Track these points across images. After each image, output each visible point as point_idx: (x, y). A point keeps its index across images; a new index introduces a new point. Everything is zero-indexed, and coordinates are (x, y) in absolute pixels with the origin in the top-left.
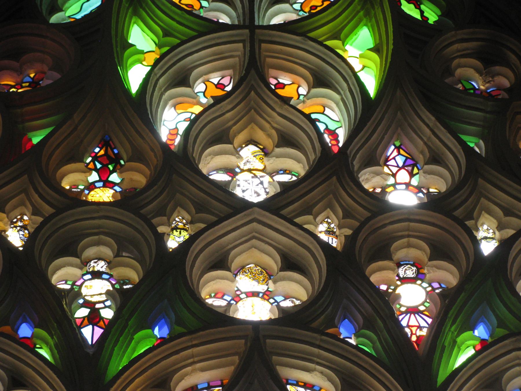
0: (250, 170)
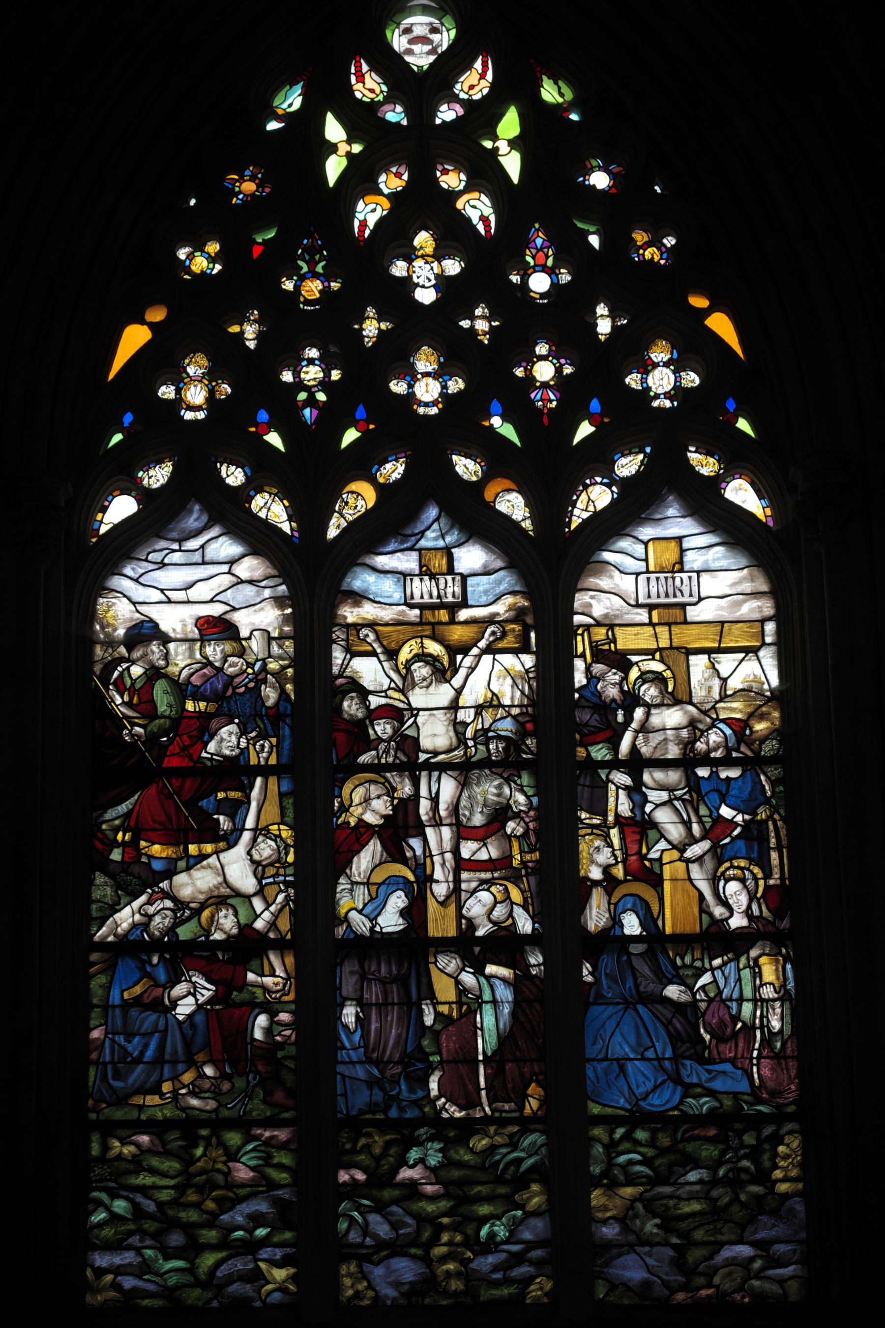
0: (422, 257)
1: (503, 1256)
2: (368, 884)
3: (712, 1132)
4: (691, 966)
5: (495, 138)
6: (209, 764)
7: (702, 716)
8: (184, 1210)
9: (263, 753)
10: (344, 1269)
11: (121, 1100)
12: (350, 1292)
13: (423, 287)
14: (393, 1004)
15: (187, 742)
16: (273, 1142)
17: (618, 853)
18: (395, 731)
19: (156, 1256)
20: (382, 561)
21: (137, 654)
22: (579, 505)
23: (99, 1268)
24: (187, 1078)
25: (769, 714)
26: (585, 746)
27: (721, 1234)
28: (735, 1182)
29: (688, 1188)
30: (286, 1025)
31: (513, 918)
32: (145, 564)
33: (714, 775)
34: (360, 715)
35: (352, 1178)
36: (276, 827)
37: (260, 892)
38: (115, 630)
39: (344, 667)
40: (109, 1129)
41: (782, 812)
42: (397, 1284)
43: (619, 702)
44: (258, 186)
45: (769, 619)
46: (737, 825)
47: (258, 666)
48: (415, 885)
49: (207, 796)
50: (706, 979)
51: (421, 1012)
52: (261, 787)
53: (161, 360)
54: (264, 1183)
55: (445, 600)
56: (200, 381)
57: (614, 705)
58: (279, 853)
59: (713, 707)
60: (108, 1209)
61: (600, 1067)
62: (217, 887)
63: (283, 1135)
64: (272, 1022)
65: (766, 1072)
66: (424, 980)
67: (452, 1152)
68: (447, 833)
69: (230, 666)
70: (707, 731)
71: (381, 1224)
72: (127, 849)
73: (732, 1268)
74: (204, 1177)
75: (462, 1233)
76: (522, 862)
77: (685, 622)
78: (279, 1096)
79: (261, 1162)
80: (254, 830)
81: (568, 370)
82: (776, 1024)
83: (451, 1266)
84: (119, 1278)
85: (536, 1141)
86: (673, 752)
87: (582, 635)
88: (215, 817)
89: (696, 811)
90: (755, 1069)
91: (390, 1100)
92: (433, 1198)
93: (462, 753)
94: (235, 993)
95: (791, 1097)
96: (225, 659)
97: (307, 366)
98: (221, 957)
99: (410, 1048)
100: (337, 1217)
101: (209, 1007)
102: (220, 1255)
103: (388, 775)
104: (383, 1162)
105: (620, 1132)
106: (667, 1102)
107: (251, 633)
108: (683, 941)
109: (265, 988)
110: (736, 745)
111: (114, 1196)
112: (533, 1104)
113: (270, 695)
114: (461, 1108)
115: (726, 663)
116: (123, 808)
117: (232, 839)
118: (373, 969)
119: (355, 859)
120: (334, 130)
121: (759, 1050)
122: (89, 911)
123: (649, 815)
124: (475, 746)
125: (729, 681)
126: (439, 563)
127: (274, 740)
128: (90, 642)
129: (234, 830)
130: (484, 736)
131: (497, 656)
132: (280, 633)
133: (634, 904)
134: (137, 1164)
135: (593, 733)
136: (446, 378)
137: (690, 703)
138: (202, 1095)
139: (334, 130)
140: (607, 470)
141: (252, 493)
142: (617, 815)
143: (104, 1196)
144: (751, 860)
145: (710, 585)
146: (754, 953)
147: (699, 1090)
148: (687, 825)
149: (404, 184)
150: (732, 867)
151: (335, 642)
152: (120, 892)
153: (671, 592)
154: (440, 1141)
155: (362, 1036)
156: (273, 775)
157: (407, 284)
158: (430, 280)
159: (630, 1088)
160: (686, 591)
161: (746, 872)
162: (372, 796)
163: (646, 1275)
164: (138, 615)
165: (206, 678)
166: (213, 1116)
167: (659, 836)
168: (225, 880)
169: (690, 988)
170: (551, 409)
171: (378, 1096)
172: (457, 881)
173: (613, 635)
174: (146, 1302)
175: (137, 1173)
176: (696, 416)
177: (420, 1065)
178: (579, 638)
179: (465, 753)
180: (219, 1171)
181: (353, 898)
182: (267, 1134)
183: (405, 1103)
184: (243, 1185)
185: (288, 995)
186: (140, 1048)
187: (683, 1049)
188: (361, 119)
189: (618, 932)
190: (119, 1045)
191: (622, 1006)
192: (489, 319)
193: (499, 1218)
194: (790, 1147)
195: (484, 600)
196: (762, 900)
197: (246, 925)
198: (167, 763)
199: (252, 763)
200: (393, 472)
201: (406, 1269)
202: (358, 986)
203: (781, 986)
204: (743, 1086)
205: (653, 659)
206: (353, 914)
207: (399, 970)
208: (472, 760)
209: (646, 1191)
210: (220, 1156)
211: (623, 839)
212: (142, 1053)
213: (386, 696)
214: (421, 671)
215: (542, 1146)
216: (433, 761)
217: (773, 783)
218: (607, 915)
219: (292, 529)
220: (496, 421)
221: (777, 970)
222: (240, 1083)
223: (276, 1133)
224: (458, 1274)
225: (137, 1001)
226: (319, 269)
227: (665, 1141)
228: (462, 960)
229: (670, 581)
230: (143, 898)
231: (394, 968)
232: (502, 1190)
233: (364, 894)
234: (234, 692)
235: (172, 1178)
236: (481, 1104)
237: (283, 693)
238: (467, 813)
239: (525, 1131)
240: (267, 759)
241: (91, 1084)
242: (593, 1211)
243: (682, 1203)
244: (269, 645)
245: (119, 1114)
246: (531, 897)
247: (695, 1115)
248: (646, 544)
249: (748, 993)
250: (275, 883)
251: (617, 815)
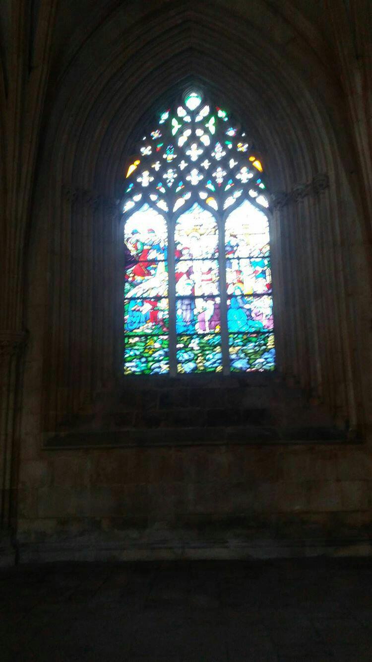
3: (255, 335)
9: (161, 257)
11: (132, 331)
12: (179, 371)
28: (260, 346)
40: (129, 337)
63: (166, 337)
92: (197, 350)
108: (249, 296)
113: (162, 245)
134: (135, 344)
139: (174, 122)
174: (137, 373)
176: (252, 184)
188: (180, 120)
194: (271, 340)
198: (142, 259)
201: (191, 365)
225: (134, 310)
227: (245, 337)
239: (216, 336)
245: (131, 334)
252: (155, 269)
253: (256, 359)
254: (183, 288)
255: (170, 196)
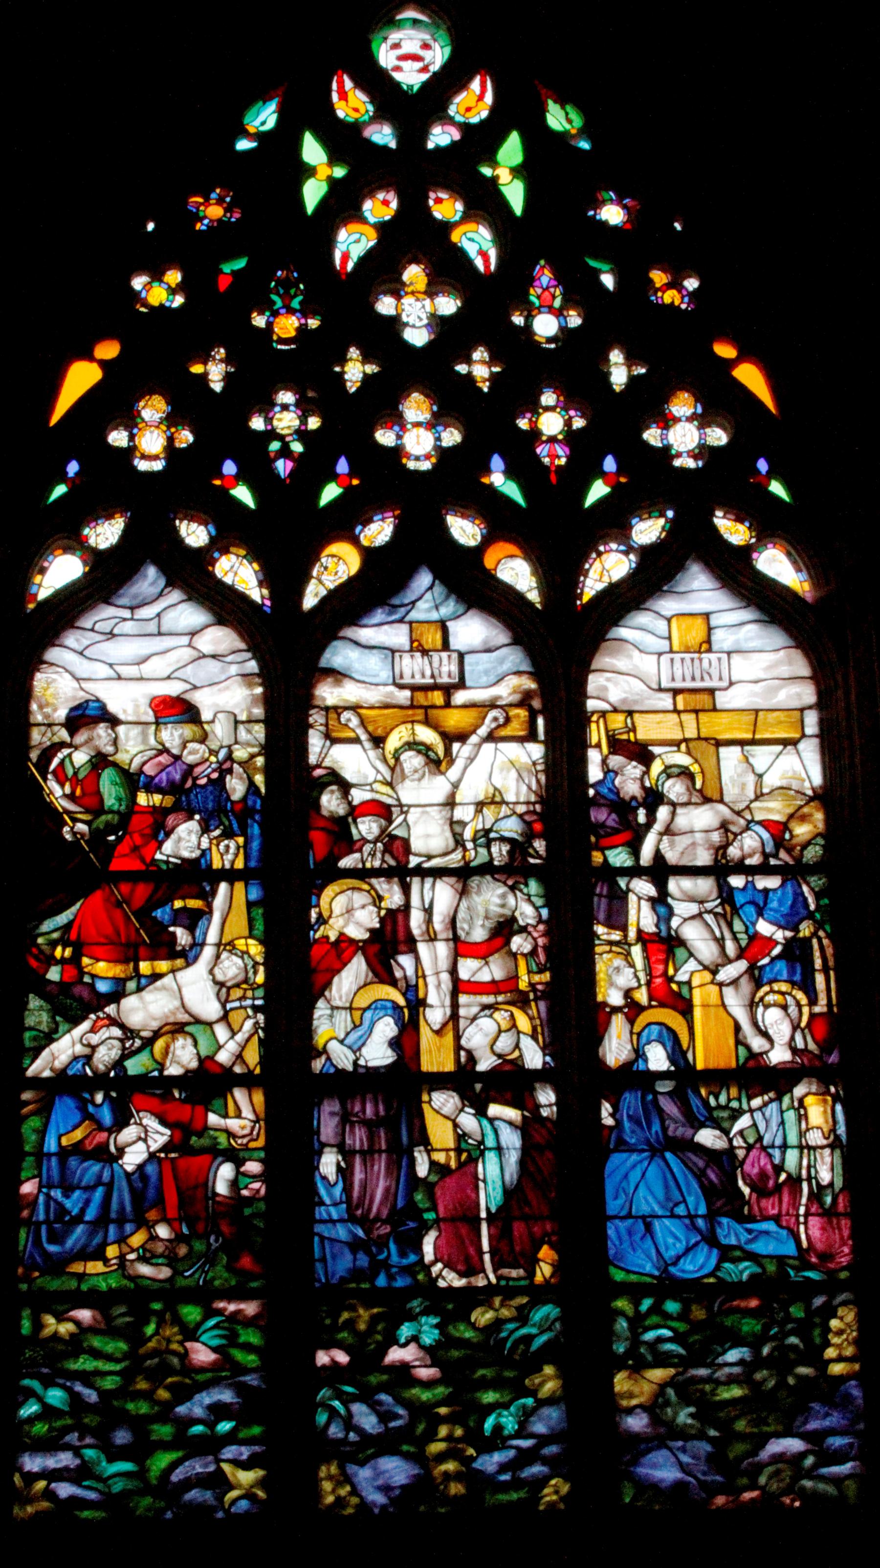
0: (413, 293)
1: (512, 1453)
2: (351, 1008)
3: (754, 1303)
4: (726, 1107)
5: (494, 164)
6: (164, 867)
7: (735, 818)
8: (132, 1401)
9: (227, 854)
10: (323, 1472)
11: (57, 1266)
12: (330, 1499)
13: (413, 326)
14: (380, 1152)
15: (138, 840)
16: (240, 1317)
17: (642, 976)
18: (383, 831)
19: (98, 1458)
20: (365, 634)
21: (80, 738)
22: (591, 574)
23: (29, 1472)
24: (137, 1239)
25: (811, 815)
26: (602, 850)
27: (768, 1425)
28: (782, 1362)
29: (727, 1370)
30: (255, 1177)
31: (520, 1050)
32: (91, 634)
33: (749, 885)
34: (341, 810)
35: (333, 1360)
36: (243, 941)
37: (225, 1018)
38: (55, 710)
39: (323, 755)
41: (828, 928)
42: (386, 1489)
43: (640, 800)
44: (226, 210)
45: (810, 707)
46: (776, 943)
47: (222, 754)
48: (406, 1011)
49: (161, 904)
50: (744, 1122)
51: (412, 1162)
52: (226, 896)
53: (112, 402)
54: (228, 1366)
55: (439, 681)
56: (157, 427)
57: (634, 804)
58: (247, 972)
59: (748, 807)
60: (40, 1400)
61: (623, 1225)
62: (174, 1014)
63: (250, 1308)
64: (238, 1173)
65: (816, 1233)
66: (417, 1122)
67: (451, 1327)
68: (443, 949)
69: (190, 753)
70: (741, 834)
71: (367, 1415)
72: (67, 967)
73: (780, 1466)
74: (156, 1360)
75: (464, 1425)
76: (532, 985)
77: (715, 709)
78: (246, 1262)
79: (224, 1342)
80: (218, 945)
81: (579, 423)
82: (825, 1176)
83: (450, 1466)
84: (53, 1485)
85: (549, 1314)
86: (704, 858)
87: (597, 722)
88: (172, 929)
89: (730, 925)
90: (802, 1228)
91: (378, 1266)
93: (460, 856)
94: (194, 1138)
95: (844, 1261)
96: (184, 746)
97: (281, 412)
98: (177, 1095)
99: (400, 1203)
100: (313, 1407)
101: (163, 1155)
102: (173, 1456)
103: (374, 881)
104: (369, 1341)
105: (646, 1304)
106: (701, 1268)
107: (215, 716)
108: (717, 1078)
109: (230, 1134)
110: (774, 851)
111: (48, 1383)
112: (544, 1271)
114: (462, 1275)
115: (762, 756)
116: (62, 919)
117: (191, 955)
118: (357, 1108)
119: (336, 980)
120: (312, 151)
121: (807, 1206)
122: (22, 1040)
123: (676, 931)
124: (475, 849)
125: (765, 778)
126: (433, 638)
127: (241, 840)
128: (25, 724)
129: (194, 945)
130: (485, 837)
131: (501, 745)
132: (248, 716)
133: (660, 1034)
134: (75, 1345)
135: (608, 835)
136: (440, 428)
137: (721, 801)
138: (154, 1261)
139: (312, 151)
140: (623, 533)
141: (216, 555)
142: (640, 932)
143: (35, 1384)
144: (793, 983)
145: (741, 668)
146: (799, 1091)
147: (738, 1253)
148: (720, 942)
149: (393, 213)
150: (772, 991)
151: (311, 726)
152: (58, 1018)
153: (698, 675)
154: (436, 1315)
155: (344, 1190)
156: (239, 880)
157: (394, 325)
158: (421, 319)
159: (658, 1252)
160: (715, 675)
161: (788, 998)
162: (356, 906)
163: (679, 1475)
164: (82, 693)
165: (161, 768)
166: (167, 1285)
167: (686, 954)
168: (183, 1005)
169: (726, 1132)
170: (559, 466)
171: (363, 1260)
172: (455, 1006)
173: (633, 723)
174: (86, 1514)
175: (76, 1356)
177: (412, 1225)
178: (593, 726)
179: (464, 857)
180: (175, 1353)
181: (333, 1025)
182: (232, 1307)
183: (394, 1270)
184: (202, 1369)
185: (256, 1140)
186: (80, 1205)
187: (719, 1204)
188: (343, 140)
189: (641, 1066)
190: (56, 1201)
191: (646, 1154)
192: (489, 364)
193: (506, 1406)
194: (843, 1321)
195: (484, 680)
196: (806, 1031)
197: (208, 1057)
198: (116, 865)
199: (215, 867)
200: (379, 533)
201: (396, 1470)
202: (339, 1130)
203: (830, 1131)
204: (790, 1249)
205: (679, 750)
206: (334, 1047)
207: (386, 1109)
208: (473, 864)
209: (677, 1374)
210: (175, 1334)
211: (647, 958)
212: (83, 1211)
213: (372, 790)
214: (412, 761)
215: (556, 1320)
216: (426, 865)
217: (818, 896)
218: (629, 1047)
219: (263, 597)
220: (498, 479)
221: (825, 1112)
222: (199, 1246)
223: (242, 1306)
224: (457, 1477)
225: (77, 1149)
226: (295, 304)
227: (699, 1313)
228: (462, 1098)
229: (697, 662)
230: (86, 1025)
231: (381, 1107)
232: (509, 1374)
233: (346, 1021)
234: (195, 785)
235: (118, 1361)
236: (483, 1271)
237: (252, 784)
238: (466, 926)
240: (233, 862)
241: (21, 1248)
242: (617, 1398)
243: (721, 1389)
244: (236, 729)
245: (55, 1285)
246: (541, 1025)
247: (733, 1283)
248: (669, 620)
249: (792, 1139)
250: (241, 1007)
251: (640, 932)
252: (192, 920)
253: (762, 1441)
254: (350, 1029)
255: (286, 536)
